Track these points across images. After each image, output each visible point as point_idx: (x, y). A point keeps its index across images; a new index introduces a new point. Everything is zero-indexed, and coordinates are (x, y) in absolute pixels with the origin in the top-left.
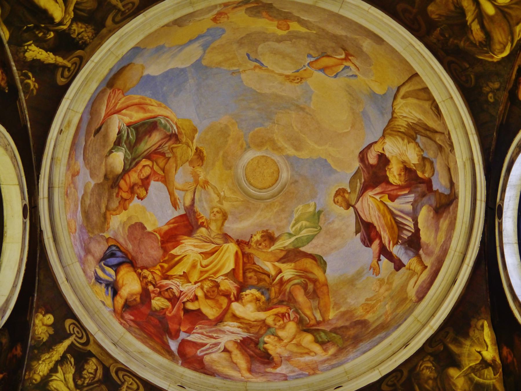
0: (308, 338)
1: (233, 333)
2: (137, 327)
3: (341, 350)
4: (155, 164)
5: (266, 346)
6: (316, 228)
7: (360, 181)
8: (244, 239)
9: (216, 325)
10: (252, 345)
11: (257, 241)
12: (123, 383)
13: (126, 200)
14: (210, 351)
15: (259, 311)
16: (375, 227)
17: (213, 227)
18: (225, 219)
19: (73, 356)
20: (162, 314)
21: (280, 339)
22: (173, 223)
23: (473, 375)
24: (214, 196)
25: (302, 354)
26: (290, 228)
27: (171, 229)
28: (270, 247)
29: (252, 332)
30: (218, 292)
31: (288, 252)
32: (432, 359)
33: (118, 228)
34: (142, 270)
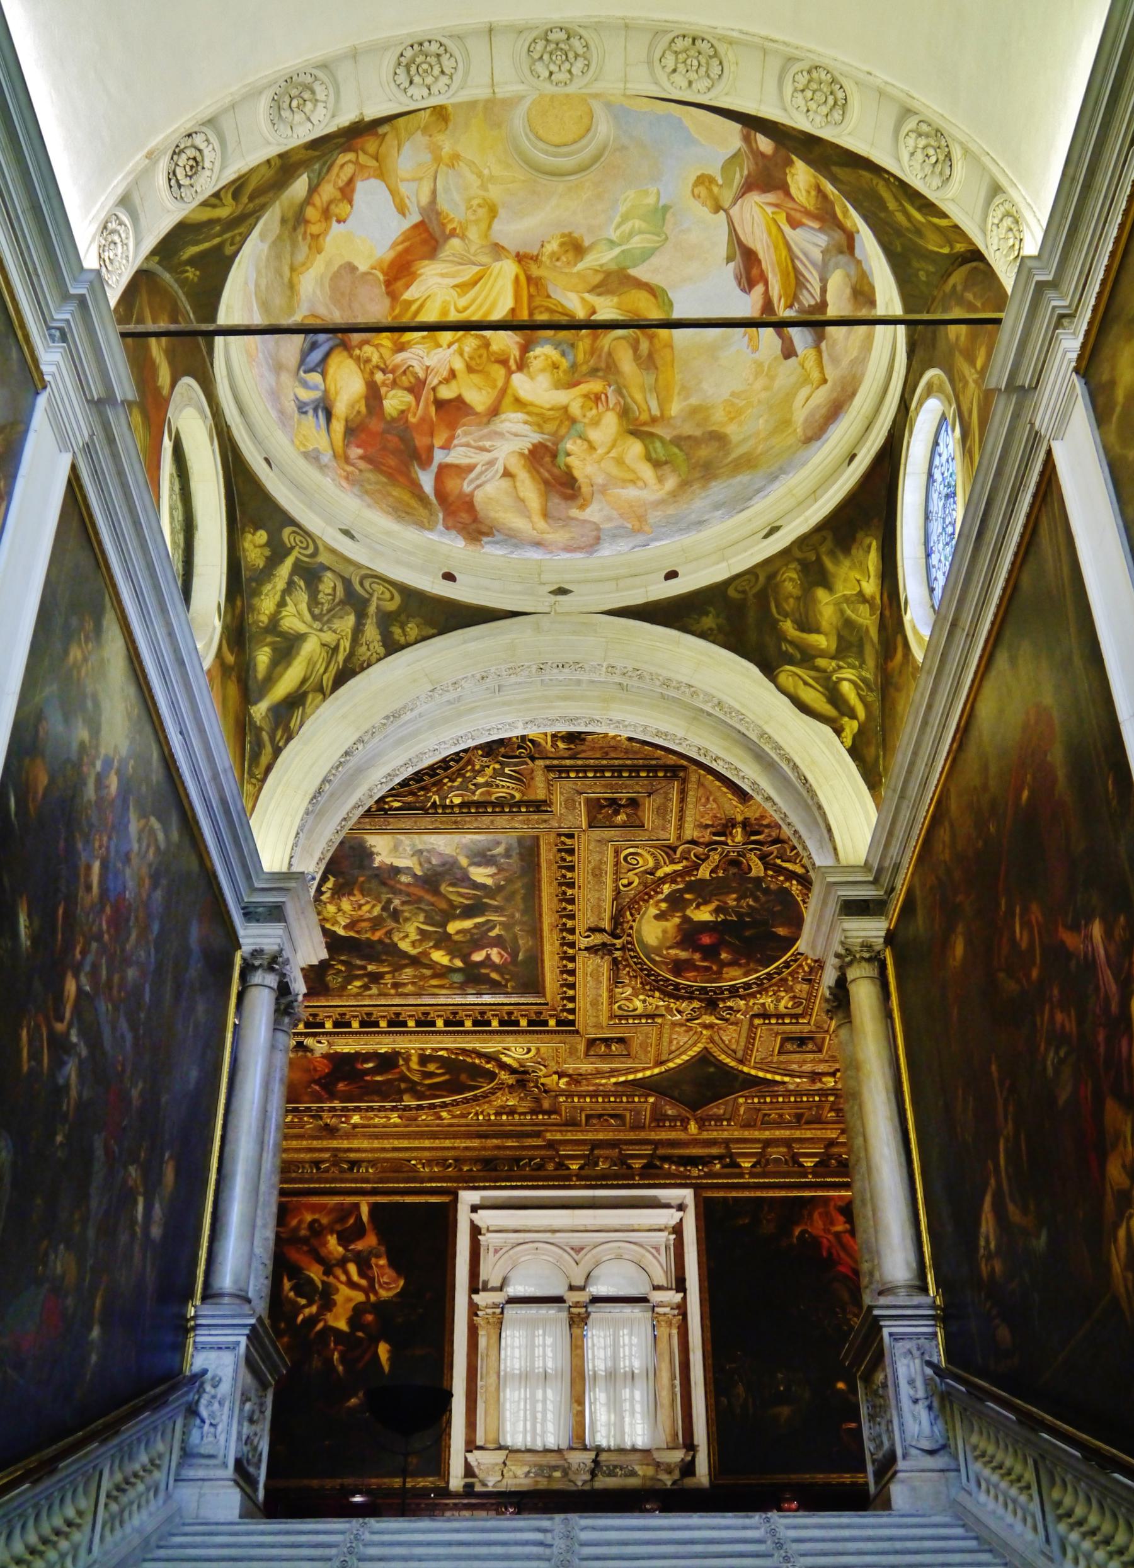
0: (636, 448)
1: (516, 435)
2: (371, 467)
3: (684, 484)
4: (360, 153)
5: (569, 460)
6: (658, 235)
7: (741, 171)
8: (528, 250)
9: (489, 422)
10: (548, 459)
11: (553, 253)
12: (371, 595)
13: (318, 236)
14: (483, 479)
15: (557, 389)
16: (759, 262)
17: (473, 234)
18: (494, 217)
19: (301, 577)
20: (402, 422)
21: (592, 447)
22: (403, 242)
23: (845, 606)
24: (472, 178)
26: (612, 231)
27: (400, 255)
28: (575, 265)
29: (546, 431)
30: (488, 358)
31: (608, 274)
32: (799, 568)
33: (314, 292)
34: (360, 349)
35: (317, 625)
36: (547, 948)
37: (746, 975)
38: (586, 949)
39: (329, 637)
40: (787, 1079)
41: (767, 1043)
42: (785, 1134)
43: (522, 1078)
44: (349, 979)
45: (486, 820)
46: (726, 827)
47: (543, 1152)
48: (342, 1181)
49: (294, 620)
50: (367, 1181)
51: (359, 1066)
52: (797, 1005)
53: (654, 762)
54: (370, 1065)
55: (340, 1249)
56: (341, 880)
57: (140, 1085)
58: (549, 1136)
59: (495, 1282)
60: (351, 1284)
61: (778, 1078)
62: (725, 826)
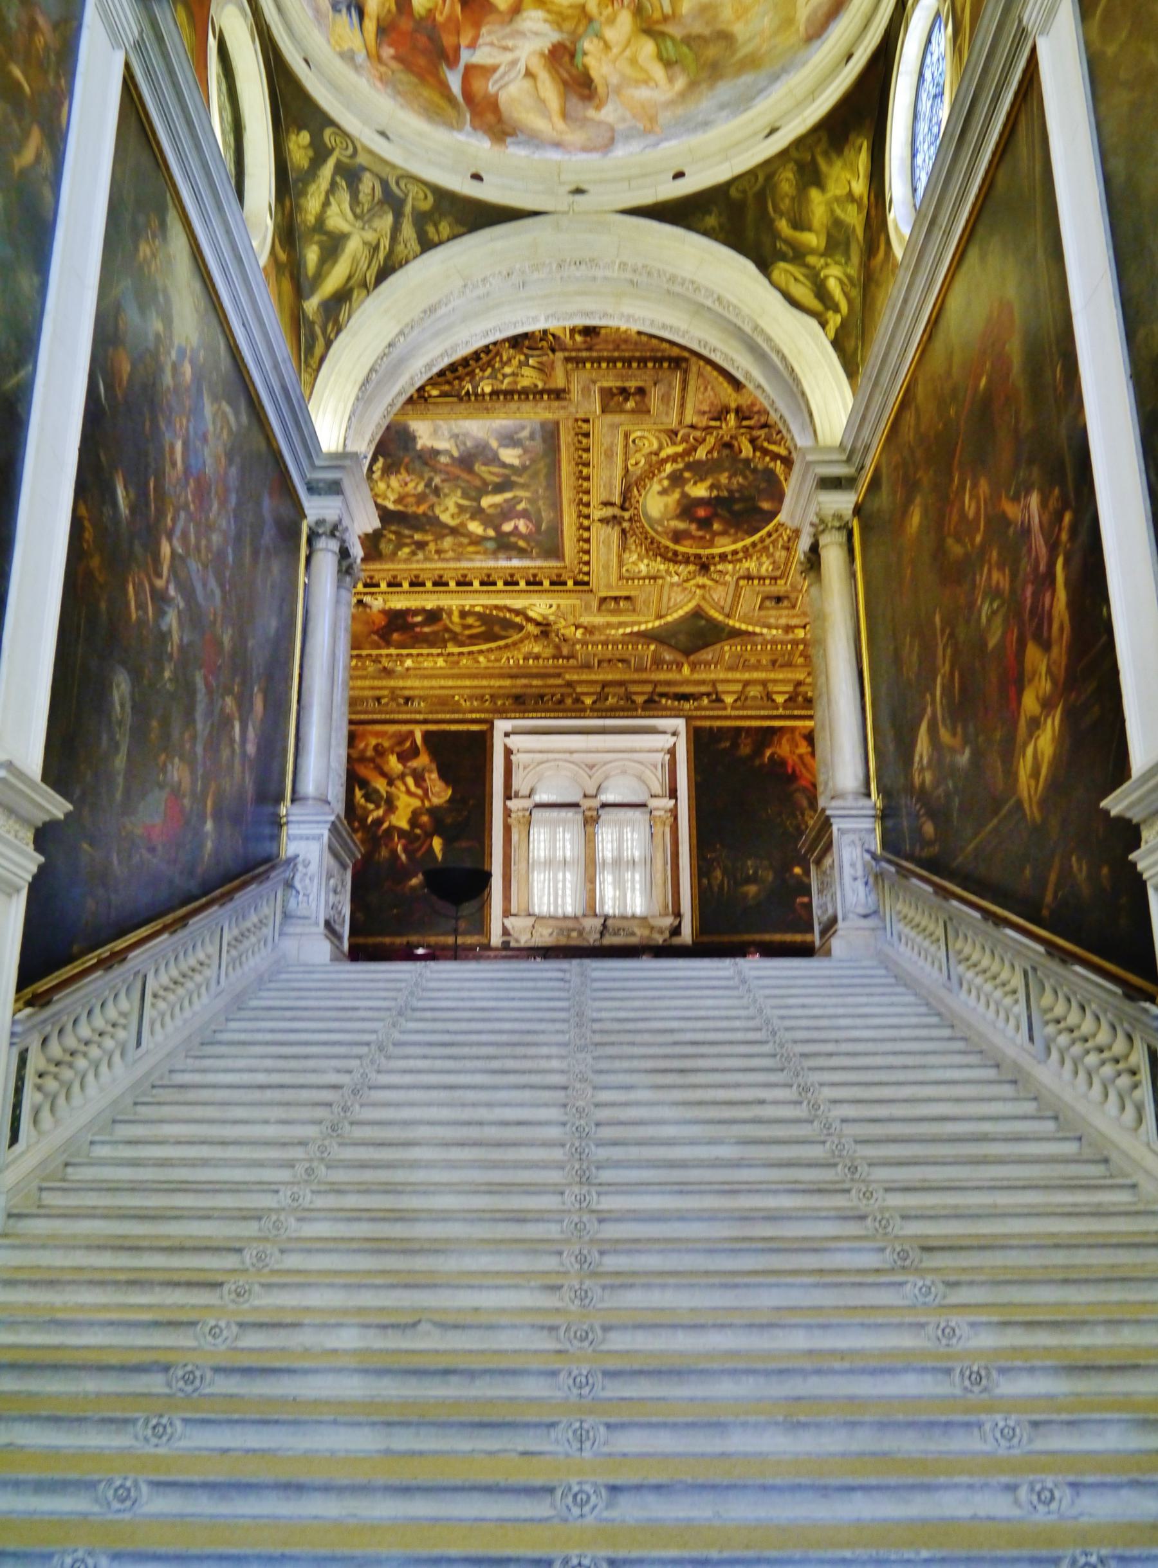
0: (648, 47)
1: (536, 34)
9: (511, 21)
10: (566, 59)
12: (406, 195)
14: (506, 79)
19: (343, 177)
21: (607, 46)
23: (835, 206)
25: (637, 83)
35: (359, 224)
36: (566, 520)
37: (734, 542)
38: (601, 520)
39: (370, 236)
40: (765, 631)
41: (750, 598)
42: (761, 675)
43: (545, 629)
44: (400, 546)
45: (513, 406)
46: (720, 414)
47: (564, 690)
48: (399, 712)
49: (339, 218)
50: (420, 712)
51: (410, 620)
52: (776, 568)
53: (659, 354)
54: (419, 619)
55: (400, 767)
56: (389, 461)
57: (230, 631)
58: (568, 677)
59: (524, 791)
60: (409, 792)
61: (758, 630)
62: (721, 413)
